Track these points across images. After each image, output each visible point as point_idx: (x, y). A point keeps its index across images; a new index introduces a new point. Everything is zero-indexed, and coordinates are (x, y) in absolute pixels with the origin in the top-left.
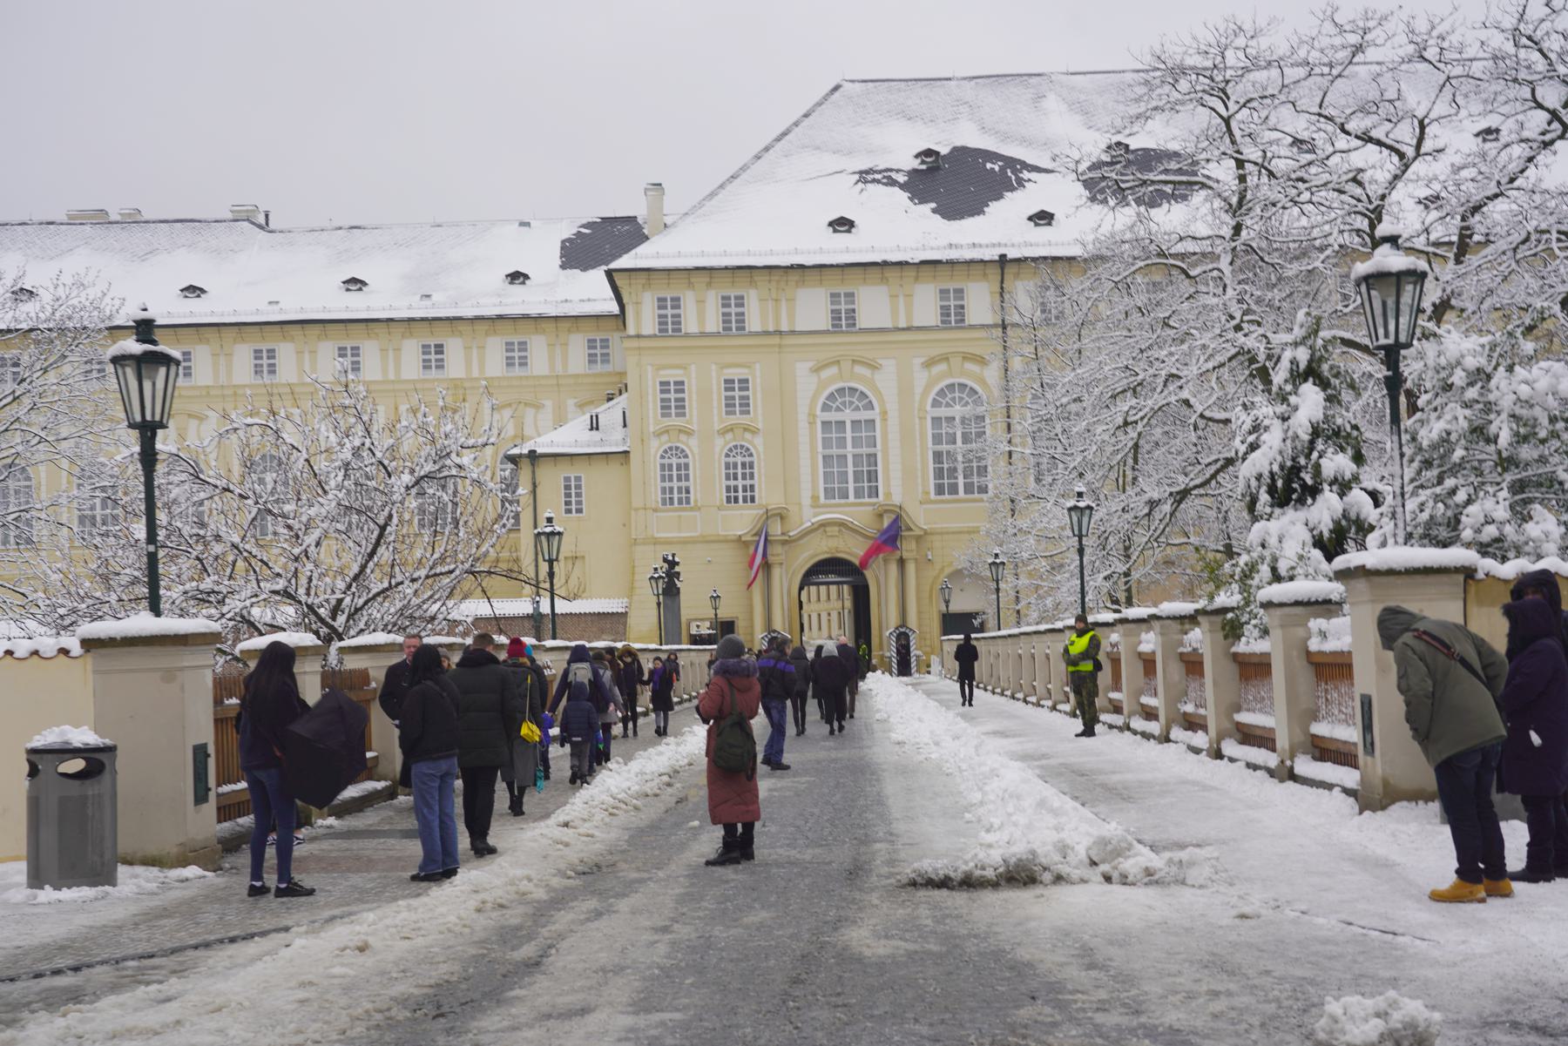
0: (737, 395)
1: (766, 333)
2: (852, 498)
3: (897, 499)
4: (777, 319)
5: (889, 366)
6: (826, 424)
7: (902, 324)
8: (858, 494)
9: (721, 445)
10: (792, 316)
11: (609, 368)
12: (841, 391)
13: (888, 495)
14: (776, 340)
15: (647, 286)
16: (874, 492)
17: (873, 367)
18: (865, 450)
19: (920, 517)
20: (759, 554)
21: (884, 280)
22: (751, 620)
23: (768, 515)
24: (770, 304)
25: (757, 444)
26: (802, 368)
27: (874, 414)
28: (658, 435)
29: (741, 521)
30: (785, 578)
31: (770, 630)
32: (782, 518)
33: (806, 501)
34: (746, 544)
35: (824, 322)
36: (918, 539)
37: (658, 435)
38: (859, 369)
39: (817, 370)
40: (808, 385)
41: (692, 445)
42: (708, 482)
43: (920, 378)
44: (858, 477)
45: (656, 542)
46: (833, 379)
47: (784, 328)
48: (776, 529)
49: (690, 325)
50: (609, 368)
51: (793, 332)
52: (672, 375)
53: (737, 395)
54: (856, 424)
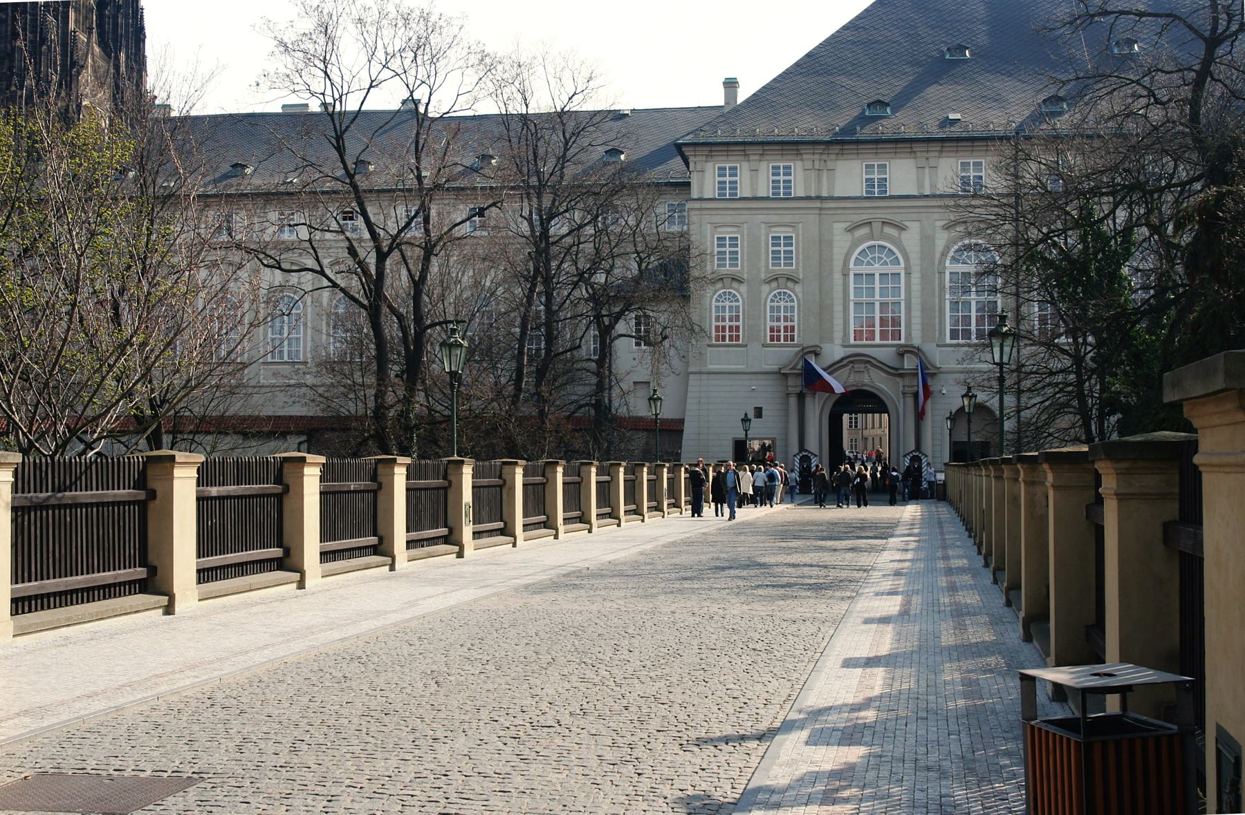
1: (808, 198)
2: (877, 341)
3: (916, 341)
5: (914, 227)
7: (927, 192)
10: (831, 185)
13: (909, 335)
14: (818, 204)
15: (710, 156)
16: (897, 335)
17: (901, 228)
24: (813, 174)
26: (839, 227)
38: (888, 230)
39: (850, 230)
43: (941, 239)
44: (883, 321)
47: (825, 194)
51: (832, 198)
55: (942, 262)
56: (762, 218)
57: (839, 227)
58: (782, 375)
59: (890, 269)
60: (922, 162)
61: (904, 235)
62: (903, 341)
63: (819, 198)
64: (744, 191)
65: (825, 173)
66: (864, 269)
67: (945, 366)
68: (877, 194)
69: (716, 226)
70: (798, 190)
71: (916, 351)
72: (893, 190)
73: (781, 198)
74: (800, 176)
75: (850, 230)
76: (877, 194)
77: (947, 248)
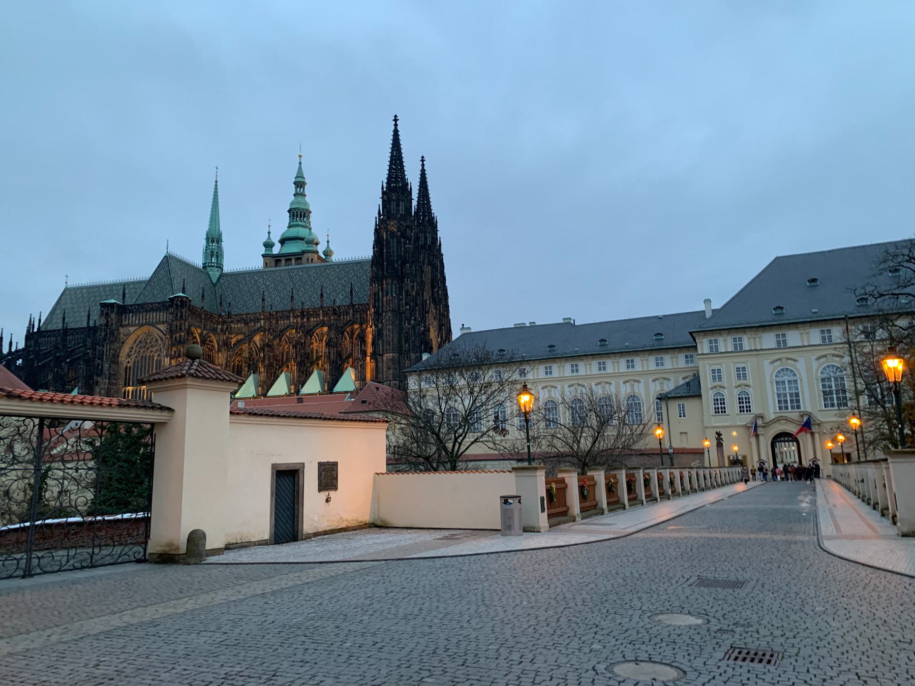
0: (741, 373)
1: (751, 350)
3: (809, 410)
4: (755, 345)
5: (802, 361)
6: (777, 383)
7: (806, 344)
8: (792, 407)
9: (736, 392)
11: (693, 365)
12: (783, 370)
16: (799, 407)
18: (794, 391)
19: (820, 417)
21: (797, 328)
22: (752, 458)
23: (757, 417)
25: (750, 391)
26: (766, 362)
28: (712, 388)
29: (747, 418)
30: (765, 442)
31: (760, 459)
32: (762, 418)
33: (771, 411)
34: (749, 428)
35: (774, 346)
36: (818, 425)
37: (712, 388)
38: (789, 362)
39: (772, 363)
40: (769, 369)
41: (725, 392)
42: (732, 406)
43: (815, 364)
44: (792, 401)
45: (714, 427)
46: (778, 366)
47: (758, 348)
48: (760, 422)
49: (722, 349)
50: (693, 365)
51: (762, 350)
52: (715, 367)
53: (741, 373)
54: (789, 382)
57: (766, 362)
58: (747, 427)
59: (792, 378)
60: (802, 331)
61: (797, 364)
62: (802, 409)
63: (756, 350)
64: (722, 349)
65: (757, 340)
66: (780, 379)
67: (823, 420)
69: (710, 365)
70: (746, 347)
71: (810, 415)
72: (789, 345)
73: (738, 349)
77: (817, 370)
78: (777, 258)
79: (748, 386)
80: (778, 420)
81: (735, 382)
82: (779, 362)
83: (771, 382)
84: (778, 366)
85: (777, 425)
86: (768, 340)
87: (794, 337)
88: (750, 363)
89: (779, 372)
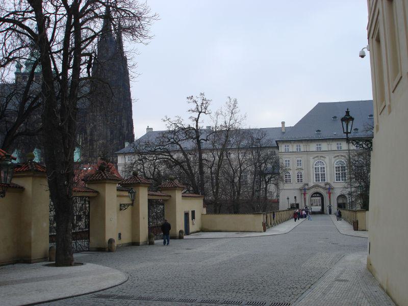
2: (320, 182)
3: (329, 182)
7: (330, 149)
9: (296, 172)
16: (324, 180)
19: (333, 185)
20: (303, 191)
25: (303, 172)
27: (325, 166)
29: (300, 185)
30: (308, 196)
32: (308, 185)
38: (322, 158)
39: (314, 158)
40: (312, 161)
43: (333, 160)
51: (309, 152)
54: (321, 168)
55: (334, 165)
56: (294, 156)
59: (322, 166)
63: (307, 151)
64: (291, 150)
67: (335, 187)
68: (319, 150)
70: (302, 150)
73: (298, 152)
74: (303, 147)
75: (314, 158)
76: (319, 150)
78: (320, 104)
79: (302, 169)
80: (313, 187)
81: (296, 167)
82: (317, 158)
83: (313, 168)
84: (317, 160)
85: (313, 189)
86: (313, 147)
87: (324, 146)
88: (303, 158)
89: (316, 163)
